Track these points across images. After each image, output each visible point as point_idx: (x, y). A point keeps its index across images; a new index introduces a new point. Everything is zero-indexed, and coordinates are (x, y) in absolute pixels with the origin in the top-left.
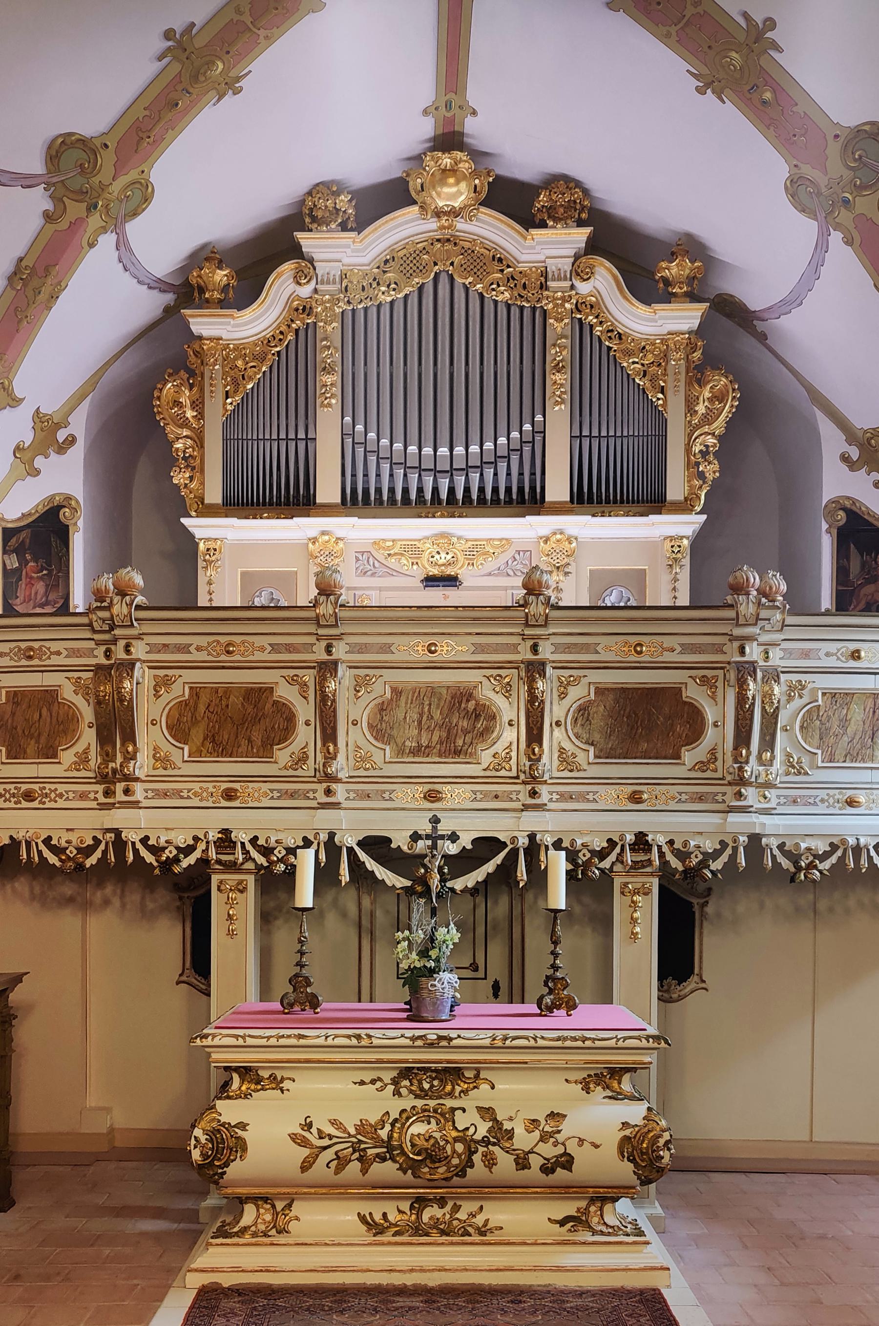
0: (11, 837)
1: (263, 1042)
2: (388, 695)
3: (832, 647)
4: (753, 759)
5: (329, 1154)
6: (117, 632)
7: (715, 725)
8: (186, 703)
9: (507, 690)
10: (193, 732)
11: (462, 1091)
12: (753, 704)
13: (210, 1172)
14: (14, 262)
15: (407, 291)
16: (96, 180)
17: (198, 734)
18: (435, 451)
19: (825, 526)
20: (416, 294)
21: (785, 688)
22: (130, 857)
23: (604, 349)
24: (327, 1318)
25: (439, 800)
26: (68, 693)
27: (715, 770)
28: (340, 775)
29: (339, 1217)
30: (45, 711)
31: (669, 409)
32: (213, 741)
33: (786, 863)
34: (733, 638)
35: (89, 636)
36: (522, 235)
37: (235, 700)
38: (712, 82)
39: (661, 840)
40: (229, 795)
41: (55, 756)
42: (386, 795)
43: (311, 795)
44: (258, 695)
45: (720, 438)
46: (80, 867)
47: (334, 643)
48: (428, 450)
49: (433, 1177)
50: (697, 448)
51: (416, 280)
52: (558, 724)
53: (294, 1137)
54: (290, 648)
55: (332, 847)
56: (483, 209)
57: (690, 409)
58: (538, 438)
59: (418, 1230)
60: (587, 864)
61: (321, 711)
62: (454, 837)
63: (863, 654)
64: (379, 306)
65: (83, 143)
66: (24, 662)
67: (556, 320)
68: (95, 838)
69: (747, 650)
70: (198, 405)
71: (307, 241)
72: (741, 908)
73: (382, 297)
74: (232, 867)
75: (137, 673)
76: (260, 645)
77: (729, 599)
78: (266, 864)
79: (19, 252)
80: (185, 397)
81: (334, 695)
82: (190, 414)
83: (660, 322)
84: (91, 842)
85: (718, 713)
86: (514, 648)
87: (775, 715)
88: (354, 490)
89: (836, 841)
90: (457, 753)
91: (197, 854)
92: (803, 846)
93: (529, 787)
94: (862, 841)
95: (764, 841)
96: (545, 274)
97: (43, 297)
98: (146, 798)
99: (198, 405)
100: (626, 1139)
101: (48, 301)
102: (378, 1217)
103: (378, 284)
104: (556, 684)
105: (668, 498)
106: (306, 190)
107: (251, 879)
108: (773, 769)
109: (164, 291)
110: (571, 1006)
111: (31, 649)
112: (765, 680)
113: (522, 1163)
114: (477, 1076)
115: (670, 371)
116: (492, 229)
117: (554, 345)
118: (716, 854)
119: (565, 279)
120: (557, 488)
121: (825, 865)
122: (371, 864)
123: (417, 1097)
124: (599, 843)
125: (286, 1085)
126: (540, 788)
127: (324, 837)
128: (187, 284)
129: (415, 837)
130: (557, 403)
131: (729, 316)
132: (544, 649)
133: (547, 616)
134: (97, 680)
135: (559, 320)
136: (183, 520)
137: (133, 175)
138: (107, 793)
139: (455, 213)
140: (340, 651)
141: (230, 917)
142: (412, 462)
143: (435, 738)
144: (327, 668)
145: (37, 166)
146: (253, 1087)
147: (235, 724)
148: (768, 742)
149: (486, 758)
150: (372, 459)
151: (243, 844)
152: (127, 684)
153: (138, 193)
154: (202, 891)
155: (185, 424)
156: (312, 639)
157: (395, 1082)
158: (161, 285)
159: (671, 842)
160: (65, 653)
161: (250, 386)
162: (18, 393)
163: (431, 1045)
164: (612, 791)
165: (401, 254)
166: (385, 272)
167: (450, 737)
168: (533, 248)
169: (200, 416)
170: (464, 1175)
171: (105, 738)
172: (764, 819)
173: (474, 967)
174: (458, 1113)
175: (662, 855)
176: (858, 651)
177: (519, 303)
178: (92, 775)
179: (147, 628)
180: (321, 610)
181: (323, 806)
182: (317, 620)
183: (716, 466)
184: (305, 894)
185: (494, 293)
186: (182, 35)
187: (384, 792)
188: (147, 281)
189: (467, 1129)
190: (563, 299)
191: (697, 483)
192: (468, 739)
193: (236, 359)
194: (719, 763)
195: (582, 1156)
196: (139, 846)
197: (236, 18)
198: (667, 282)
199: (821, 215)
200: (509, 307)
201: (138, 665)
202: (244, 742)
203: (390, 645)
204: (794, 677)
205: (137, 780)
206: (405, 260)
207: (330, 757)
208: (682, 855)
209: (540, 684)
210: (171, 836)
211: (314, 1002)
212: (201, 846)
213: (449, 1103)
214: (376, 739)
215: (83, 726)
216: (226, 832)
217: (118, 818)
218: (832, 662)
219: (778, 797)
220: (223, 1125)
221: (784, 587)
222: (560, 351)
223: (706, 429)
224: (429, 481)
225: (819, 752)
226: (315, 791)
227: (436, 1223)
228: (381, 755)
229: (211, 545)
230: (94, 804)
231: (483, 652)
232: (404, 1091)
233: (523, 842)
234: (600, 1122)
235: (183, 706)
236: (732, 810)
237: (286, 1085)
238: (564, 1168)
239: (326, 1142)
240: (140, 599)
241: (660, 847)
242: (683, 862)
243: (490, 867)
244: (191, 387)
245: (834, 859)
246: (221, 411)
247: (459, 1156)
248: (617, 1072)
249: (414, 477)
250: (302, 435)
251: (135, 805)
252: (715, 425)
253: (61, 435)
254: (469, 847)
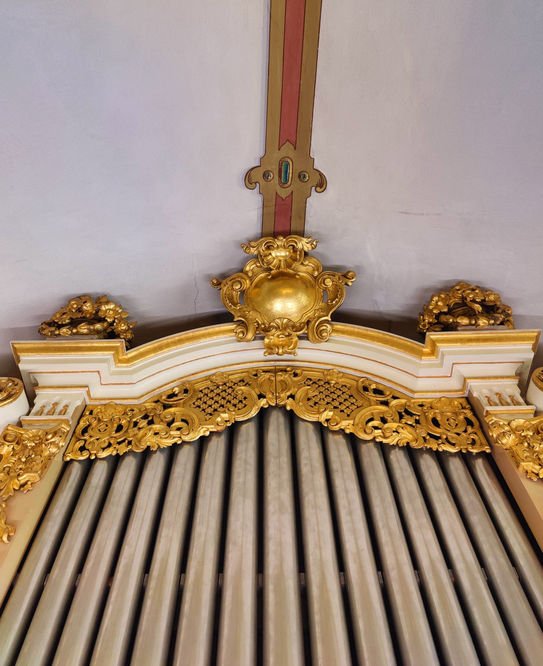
15: (203, 431)
36: (411, 350)
51: (225, 416)
96: (470, 402)
166: (166, 407)
177: (434, 445)
185: (378, 432)
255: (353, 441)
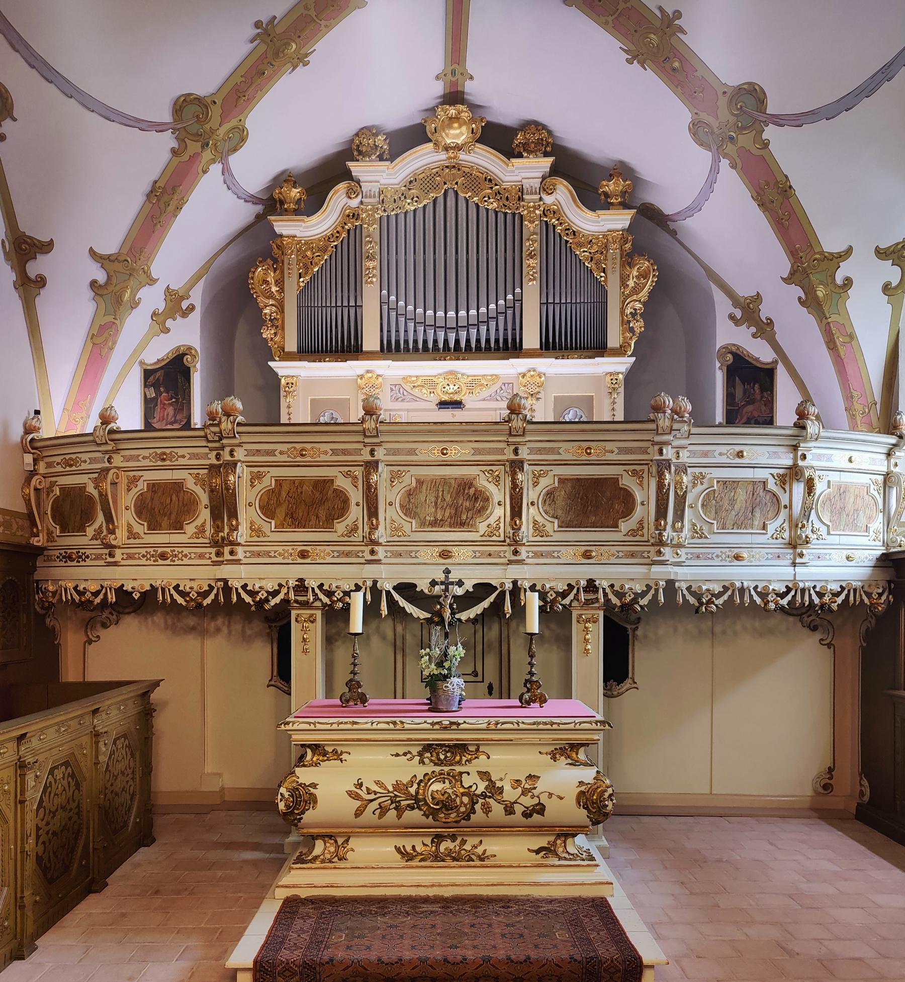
0: (151, 585)
1: (328, 727)
2: (414, 484)
3: (723, 449)
4: (669, 528)
5: (375, 805)
6: (224, 441)
7: (642, 504)
8: (273, 491)
9: (497, 480)
10: (278, 511)
11: (467, 760)
12: (669, 489)
13: (292, 818)
14: (151, 184)
15: (425, 202)
16: (208, 126)
17: (281, 512)
18: (446, 314)
19: (718, 365)
20: (432, 205)
21: (691, 478)
22: (235, 599)
23: (563, 242)
24: (374, 919)
25: (450, 557)
26: (190, 484)
27: (643, 536)
28: (380, 541)
29: (381, 849)
30: (174, 497)
31: (609, 283)
32: (292, 517)
33: (692, 600)
34: (654, 443)
35: (204, 444)
37: (307, 489)
38: (636, 56)
39: (605, 584)
40: (303, 555)
41: (181, 528)
42: (413, 554)
43: (360, 554)
44: (322, 485)
45: (645, 304)
46: (200, 605)
47: (376, 448)
48: (440, 314)
49: (446, 820)
50: (628, 311)
52: (532, 504)
53: (350, 793)
54: (345, 452)
55: (375, 590)
56: (478, 145)
57: (624, 284)
58: (518, 304)
59: (437, 857)
60: (554, 601)
61: (367, 496)
62: (460, 583)
63: (745, 454)
64: (406, 213)
65: (198, 100)
66: (159, 463)
67: (530, 222)
68: (209, 585)
69: (664, 451)
70: (280, 283)
71: (355, 168)
72: (661, 632)
73: (408, 207)
74: (306, 605)
75: (238, 470)
76: (324, 450)
77: (652, 416)
78: (329, 603)
79: (154, 177)
80: (271, 278)
81: (376, 485)
82: (274, 289)
83: (602, 223)
84: (207, 588)
85: (644, 496)
86: (501, 451)
87: (684, 497)
88: (389, 342)
89: (727, 584)
90: (462, 524)
91: (281, 596)
92: (704, 588)
93: (513, 548)
94: (746, 584)
95: (677, 584)
96: (521, 190)
97: (171, 208)
98: (245, 557)
99: (280, 283)
100: (582, 793)
101: (175, 211)
102: (409, 849)
103: (405, 198)
104: (531, 476)
105: (609, 346)
106: (354, 132)
107: (319, 614)
108: (683, 535)
109: (256, 204)
110: (542, 701)
111: (164, 454)
112: (677, 472)
113: (509, 810)
114: (477, 750)
115: (609, 257)
116: (484, 159)
117: (528, 240)
118: (644, 594)
119: (536, 193)
120: (531, 339)
121: (720, 601)
122: (402, 603)
123: (436, 764)
124: (561, 587)
125: (344, 756)
126: (519, 548)
127: (369, 583)
128: (271, 198)
129: (433, 583)
130: (530, 280)
131: (650, 218)
132: (522, 452)
133: (524, 428)
134: (210, 475)
135: (532, 222)
136: (269, 363)
137: (233, 123)
138: (218, 554)
139: (458, 148)
140: (380, 454)
141: (304, 640)
142: (430, 321)
143: (447, 514)
144: (371, 466)
145: (166, 117)
146: (321, 758)
147: (307, 505)
148: (679, 516)
149: (482, 527)
150: (402, 320)
151: (313, 589)
152: (231, 478)
153: (237, 136)
154: (285, 622)
155: (271, 296)
156: (360, 446)
157: (420, 754)
158: (253, 199)
159: (612, 586)
160: (188, 456)
161: (316, 270)
162: (154, 276)
163: (445, 728)
164: (571, 550)
165: (421, 176)
167: (457, 513)
168: (513, 172)
169: (282, 290)
170: (469, 819)
171: (216, 515)
172: (676, 569)
173: (475, 674)
174: (464, 775)
175: (605, 595)
176: (742, 452)
178: (207, 541)
179: (245, 438)
180: (366, 425)
181: (369, 562)
182: (364, 433)
183: (642, 324)
184: (357, 624)
186: (267, 25)
187: (411, 552)
188: (244, 197)
189: (471, 787)
190: (535, 208)
191: (628, 335)
192: (470, 515)
193: (306, 250)
194: (645, 531)
195: (551, 805)
196: (240, 590)
197: (305, 12)
198: (607, 195)
199: (714, 148)
200: (496, 213)
201: (239, 464)
202: (313, 518)
203: (415, 450)
204: (697, 471)
205: (239, 544)
206: (423, 181)
207: (373, 528)
208: (620, 595)
209: (520, 476)
210: (263, 583)
211: (363, 699)
212: (284, 591)
213: (458, 769)
214: (405, 515)
215: (201, 507)
216: (301, 580)
217: (225, 571)
218: (724, 460)
219: (687, 554)
220: (300, 785)
221: (689, 408)
222: (532, 244)
223: (635, 297)
224: (441, 335)
225: (715, 522)
226: (363, 552)
227: (449, 853)
228: (409, 526)
229: (289, 380)
230: (209, 562)
231: (480, 454)
232: (426, 761)
233: (509, 586)
234: (563, 781)
235: (270, 493)
236: (654, 563)
237: (344, 756)
238: (538, 813)
239: (372, 796)
240: (240, 419)
241: (604, 589)
242: (620, 600)
243: (486, 604)
244: (275, 270)
245: (725, 597)
246: (296, 287)
247: (465, 805)
248: (575, 746)
249: (431, 332)
250: (352, 303)
251: (238, 562)
252: (641, 295)
253: (185, 305)
254: (471, 590)
255: (477, 206)
